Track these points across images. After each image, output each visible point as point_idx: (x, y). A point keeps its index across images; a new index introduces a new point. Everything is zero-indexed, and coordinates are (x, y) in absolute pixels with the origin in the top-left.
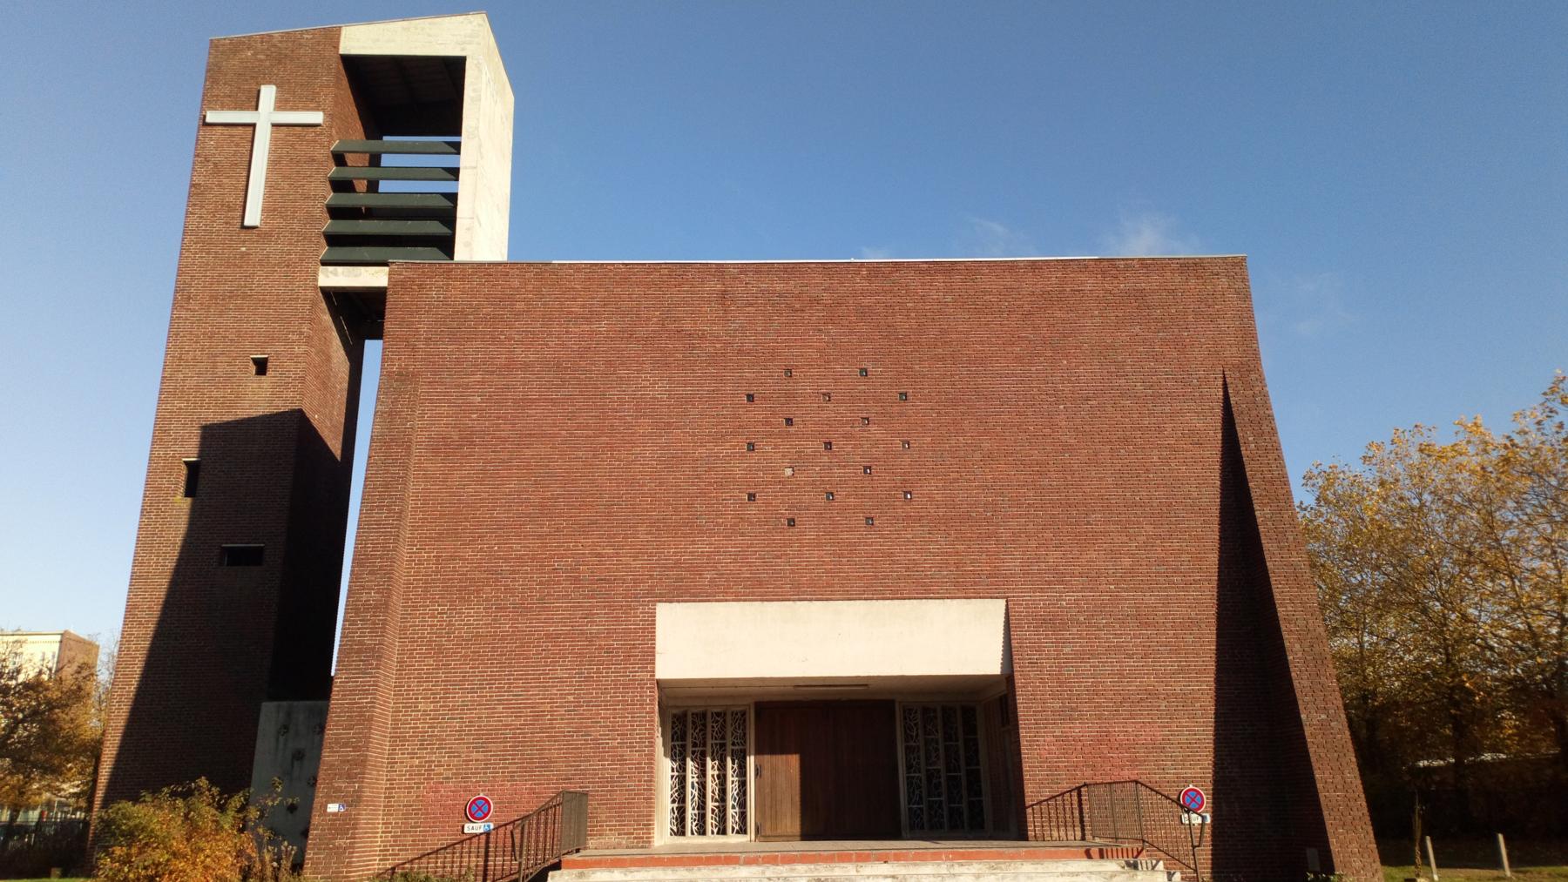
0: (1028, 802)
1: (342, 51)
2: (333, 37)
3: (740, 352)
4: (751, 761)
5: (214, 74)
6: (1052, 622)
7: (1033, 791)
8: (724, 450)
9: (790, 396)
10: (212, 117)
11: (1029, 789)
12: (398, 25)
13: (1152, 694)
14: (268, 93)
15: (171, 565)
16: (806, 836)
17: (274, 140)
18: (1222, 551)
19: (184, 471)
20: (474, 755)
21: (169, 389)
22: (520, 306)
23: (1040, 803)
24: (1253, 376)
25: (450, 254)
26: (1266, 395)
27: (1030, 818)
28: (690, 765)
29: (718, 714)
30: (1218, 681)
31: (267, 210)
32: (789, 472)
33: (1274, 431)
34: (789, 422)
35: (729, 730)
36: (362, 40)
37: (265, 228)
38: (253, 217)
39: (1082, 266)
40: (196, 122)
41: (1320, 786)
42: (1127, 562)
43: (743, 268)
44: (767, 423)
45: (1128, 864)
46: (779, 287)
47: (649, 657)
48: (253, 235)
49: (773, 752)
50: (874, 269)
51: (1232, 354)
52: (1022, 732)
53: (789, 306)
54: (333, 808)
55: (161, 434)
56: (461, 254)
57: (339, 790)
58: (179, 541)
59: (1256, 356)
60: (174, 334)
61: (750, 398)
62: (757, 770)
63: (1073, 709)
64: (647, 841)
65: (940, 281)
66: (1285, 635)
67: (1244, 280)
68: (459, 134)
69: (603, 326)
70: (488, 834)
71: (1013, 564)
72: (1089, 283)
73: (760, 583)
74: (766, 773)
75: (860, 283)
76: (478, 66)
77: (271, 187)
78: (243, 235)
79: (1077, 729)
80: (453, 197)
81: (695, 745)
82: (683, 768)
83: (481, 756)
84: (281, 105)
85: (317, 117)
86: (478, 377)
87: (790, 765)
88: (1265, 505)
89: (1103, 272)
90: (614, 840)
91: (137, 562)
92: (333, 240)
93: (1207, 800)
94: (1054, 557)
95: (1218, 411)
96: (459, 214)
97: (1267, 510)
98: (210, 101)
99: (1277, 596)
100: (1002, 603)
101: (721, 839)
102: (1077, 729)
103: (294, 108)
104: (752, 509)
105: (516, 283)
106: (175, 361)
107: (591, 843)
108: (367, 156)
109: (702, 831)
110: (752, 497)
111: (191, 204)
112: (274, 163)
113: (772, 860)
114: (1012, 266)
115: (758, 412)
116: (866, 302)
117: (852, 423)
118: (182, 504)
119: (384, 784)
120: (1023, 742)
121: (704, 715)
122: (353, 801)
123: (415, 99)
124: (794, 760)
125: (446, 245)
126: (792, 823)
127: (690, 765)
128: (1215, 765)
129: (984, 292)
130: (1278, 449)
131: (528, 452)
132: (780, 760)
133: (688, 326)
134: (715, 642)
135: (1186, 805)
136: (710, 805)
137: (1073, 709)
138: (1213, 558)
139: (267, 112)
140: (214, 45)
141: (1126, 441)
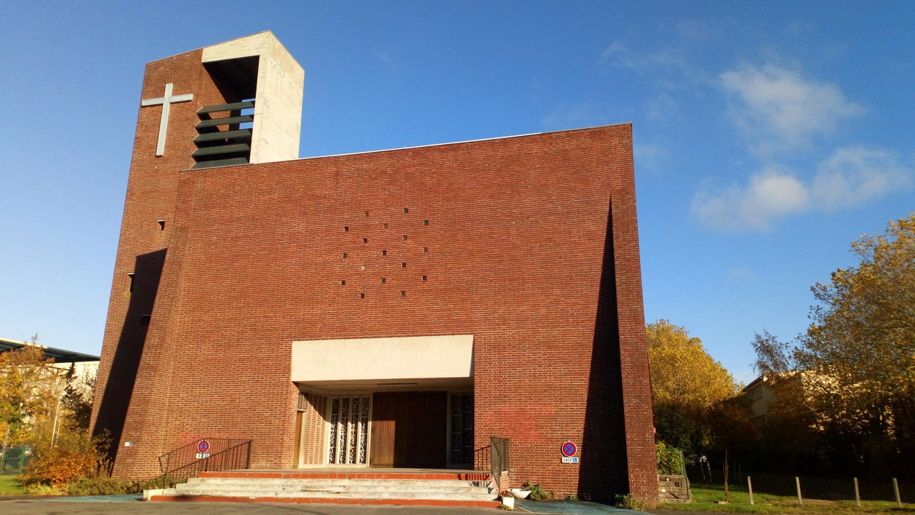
0: (476, 448)
1: (203, 61)
2: (199, 53)
3: (343, 204)
4: (370, 424)
5: (147, 81)
6: (498, 347)
7: (480, 440)
8: (330, 258)
9: (367, 226)
10: (144, 103)
11: (477, 441)
12: (228, 44)
13: (550, 387)
14: (169, 88)
15: (121, 325)
16: (397, 465)
17: (171, 111)
18: (600, 303)
19: (130, 279)
20: (203, 420)
21: (123, 242)
22: (237, 188)
23: (482, 449)
24: (628, 197)
25: (248, 160)
26: (635, 208)
27: (476, 458)
28: (340, 426)
29: (356, 399)
30: (591, 379)
31: (167, 147)
32: (363, 268)
33: (636, 229)
34: (366, 240)
35: (361, 408)
36: (214, 53)
37: (166, 156)
38: (160, 151)
39: (533, 139)
40: (138, 106)
41: (628, 442)
42: (543, 311)
43: (348, 158)
44: (354, 242)
45: (474, 483)
46: (365, 166)
47: (287, 370)
48: (160, 160)
49: (381, 419)
50: (416, 152)
51: (618, 184)
52: (476, 409)
53: (370, 177)
54: (127, 444)
55: (119, 263)
56: (253, 160)
57: (131, 436)
58: (125, 314)
59: (632, 183)
60: (126, 212)
61: (347, 229)
62: (445, 429)
63: (505, 397)
64: (280, 465)
65: (452, 153)
66: (622, 352)
67: (630, 138)
68: (254, 97)
70: (207, 459)
71: (478, 315)
72: (535, 149)
73: (345, 329)
74: (378, 432)
75: (408, 160)
76: (265, 59)
77: (169, 134)
78: (157, 161)
79: (505, 407)
80: (251, 130)
81: (344, 416)
82: (336, 428)
83: (206, 420)
84: (176, 92)
85: (190, 97)
87: (392, 424)
88: (623, 274)
89: (544, 142)
90: (264, 464)
91: (108, 325)
92: (198, 158)
93: (578, 449)
94: (501, 310)
95: (606, 219)
96: (253, 139)
97: (623, 277)
98: (145, 95)
99: (621, 329)
100: (471, 337)
101: (353, 466)
102: (505, 407)
103: (180, 94)
104: (343, 290)
106: (126, 226)
107: (253, 465)
108: (229, 112)
110: (344, 283)
112: (171, 122)
113: (379, 476)
114: (492, 143)
115: (349, 237)
116: (410, 171)
117: (398, 239)
118: (127, 294)
119: (163, 433)
120: (476, 415)
121: (325, 399)
122: (136, 441)
123: (237, 80)
124: (392, 424)
125: (246, 155)
126: (389, 458)
127: (340, 426)
128: (585, 429)
129: (476, 159)
130: (637, 240)
132: (385, 423)
133: (318, 192)
134: (321, 360)
135: (568, 450)
136: (349, 447)
137: (505, 397)
138: (595, 307)
139: (169, 95)
140: (147, 66)
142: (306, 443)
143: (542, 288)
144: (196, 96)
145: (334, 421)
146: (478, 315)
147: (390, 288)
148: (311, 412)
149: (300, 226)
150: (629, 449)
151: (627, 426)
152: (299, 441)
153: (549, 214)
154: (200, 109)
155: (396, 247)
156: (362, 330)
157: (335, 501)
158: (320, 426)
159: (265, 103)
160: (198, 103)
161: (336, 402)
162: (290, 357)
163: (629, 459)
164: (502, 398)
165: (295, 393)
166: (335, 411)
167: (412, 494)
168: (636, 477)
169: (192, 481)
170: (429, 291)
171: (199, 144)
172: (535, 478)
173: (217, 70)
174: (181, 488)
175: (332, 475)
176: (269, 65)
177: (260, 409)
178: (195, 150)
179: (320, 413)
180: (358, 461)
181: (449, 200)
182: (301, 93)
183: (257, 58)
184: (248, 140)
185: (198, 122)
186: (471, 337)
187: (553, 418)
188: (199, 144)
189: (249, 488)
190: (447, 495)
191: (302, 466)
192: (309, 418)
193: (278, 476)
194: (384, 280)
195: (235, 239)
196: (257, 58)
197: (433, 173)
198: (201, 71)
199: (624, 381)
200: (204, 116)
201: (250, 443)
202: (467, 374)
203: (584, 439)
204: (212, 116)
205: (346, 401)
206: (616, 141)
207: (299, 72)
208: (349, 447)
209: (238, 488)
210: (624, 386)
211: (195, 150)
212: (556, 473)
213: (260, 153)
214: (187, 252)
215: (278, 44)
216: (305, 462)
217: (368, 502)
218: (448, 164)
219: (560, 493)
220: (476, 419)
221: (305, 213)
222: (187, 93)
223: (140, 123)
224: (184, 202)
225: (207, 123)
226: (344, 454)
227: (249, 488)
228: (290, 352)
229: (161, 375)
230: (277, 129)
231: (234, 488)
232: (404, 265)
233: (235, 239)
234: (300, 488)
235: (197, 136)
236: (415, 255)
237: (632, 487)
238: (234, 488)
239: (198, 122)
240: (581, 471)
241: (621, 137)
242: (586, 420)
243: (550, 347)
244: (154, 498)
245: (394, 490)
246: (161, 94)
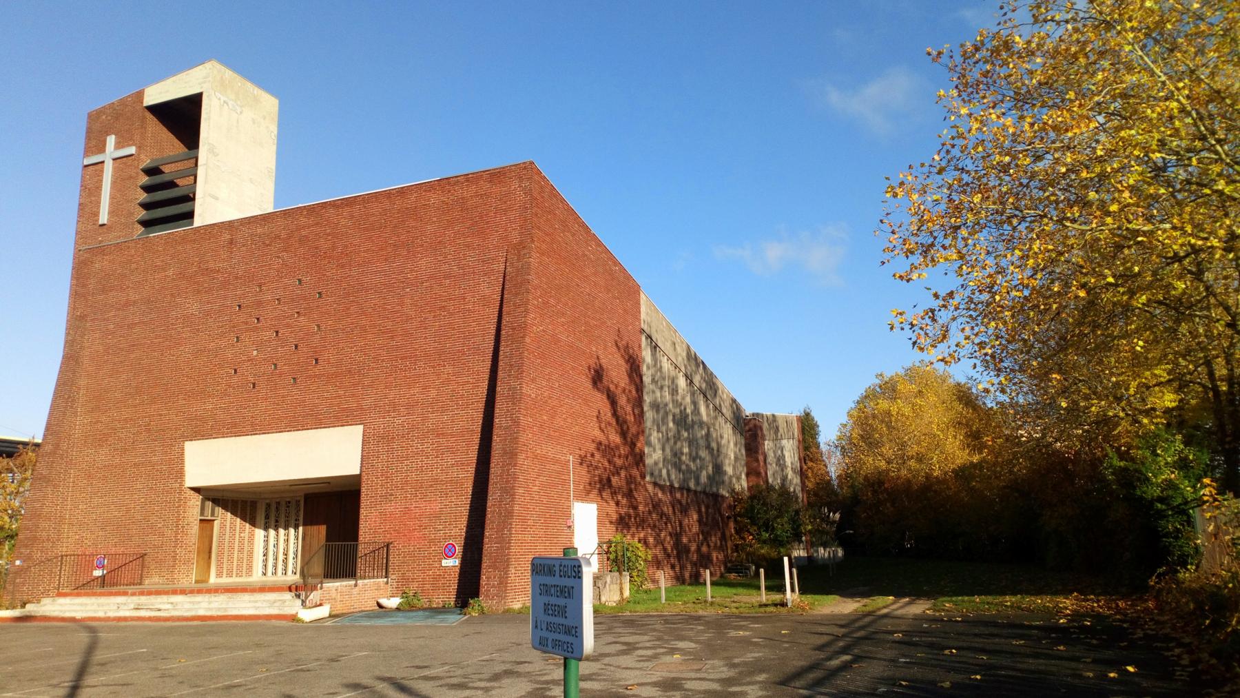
1: (145, 104)
2: (140, 95)
3: (237, 278)
9: (259, 304)
10: (86, 163)
12: (170, 81)
14: (111, 140)
17: (114, 168)
22: (134, 266)
32: (255, 353)
36: (158, 94)
38: (104, 218)
39: (429, 187)
41: (486, 540)
44: (246, 323)
46: (259, 231)
47: (180, 474)
50: (311, 210)
52: (362, 511)
56: (198, 222)
65: (347, 209)
66: (495, 437)
69: (170, 273)
72: (434, 199)
73: (235, 425)
74: (308, 538)
75: (303, 220)
77: (112, 198)
79: (389, 508)
84: (118, 146)
86: (112, 314)
87: (323, 529)
92: (147, 224)
93: (459, 550)
99: (497, 411)
101: (284, 578)
102: (389, 508)
103: (123, 147)
104: (235, 379)
105: (133, 252)
107: (147, 582)
109: (275, 573)
111: (80, 216)
112: (114, 183)
116: (303, 233)
125: (190, 215)
131: (132, 356)
133: (211, 265)
134: (216, 461)
140: (90, 116)
142: (218, 556)
143: (433, 367)
144: (139, 148)
145: (266, 529)
146: (368, 402)
147: (280, 375)
148: (224, 520)
149: (193, 307)
151: (487, 522)
152: (210, 552)
153: (445, 278)
154: (146, 162)
155: (288, 326)
156: (252, 425)
157: (150, 619)
158: (246, 535)
159: (212, 150)
160: (142, 156)
161: (268, 505)
162: (183, 460)
163: (485, 559)
164: (386, 497)
165: (196, 500)
166: (267, 517)
167: (225, 609)
169: (45, 601)
171: (146, 206)
174: (31, 608)
175: (263, 589)
177: (153, 519)
178: (142, 214)
179: (244, 519)
181: (343, 267)
182: (274, 129)
184: (190, 198)
185: (145, 180)
186: (361, 427)
187: (437, 516)
188: (146, 206)
189: (89, 608)
191: (213, 579)
192: (223, 526)
193: (175, 592)
194: (276, 365)
195: (131, 326)
197: (328, 235)
198: (144, 117)
199: (492, 471)
200: (152, 171)
201: (388, 546)
202: (358, 472)
203: (466, 538)
204: (166, 169)
205: (278, 503)
207: (270, 103)
208: (281, 557)
209: (78, 608)
210: (492, 476)
211: (142, 214)
212: (436, 578)
215: (228, 74)
216: (219, 575)
218: (343, 222)
219: (437, 601)
220: (361, 522)
221: (199, 292)
222: (129, 145)
223: (84, 187)
224: (84, 286)
225: (158, 179)
226: (275, 566)
227: (89, 608)
228: (183, 454)
229: (55, 486)
230: (237, 177)
232: (296, 346)
233: (131, 326)
234: (132, 606)
235: (143, 196)
237: (482, 590)
238: (74, 608)
239: (145, 180)
240: (460, 575)
241: (521, 179)
246: (101, 149)
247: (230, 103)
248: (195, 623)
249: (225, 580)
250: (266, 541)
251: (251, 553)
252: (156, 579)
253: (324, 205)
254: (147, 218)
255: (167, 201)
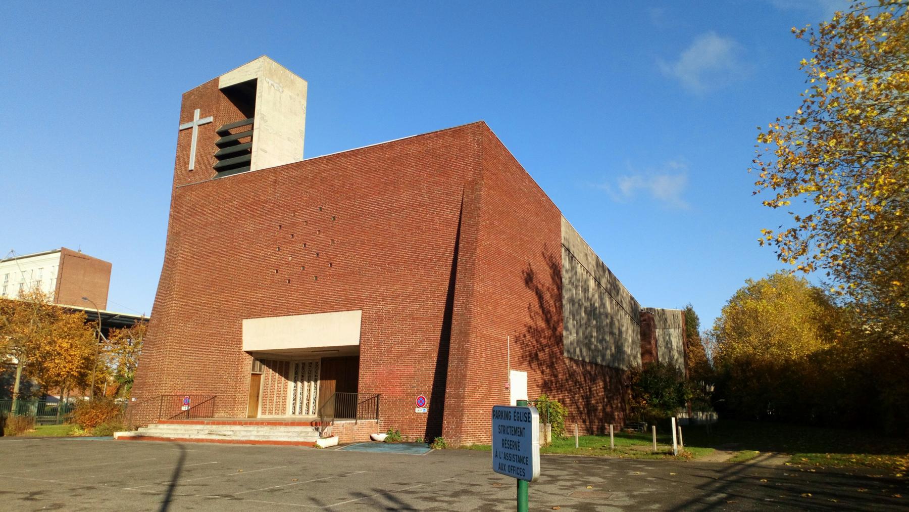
2: (216, 81)
6: (378, 320)
8: (269, 252)
9: (294, 224)
10: (181, 128)
13: (412, 352)
14: (197, 113)
24: (478, 186)
31: (197, 162)
36: (229, 79)
38: (192, 166)
39: (410, 141)
41: (447, 395)
42: (410, 288)
47: (239, 342)
50: (329, 158)
52: (360, 371)
56: (253, 168)
65: (353, 158)
66: (454, 321)
69: (235, 203)
71: (365, 294)
72: (412, 149)
73: (276, 309)
74: (323, 389)
77: (197, 152)
84: (202, 116)
85: (211, 119)
92: (220, 169)
93: (427, 401)
94: (381, 289)
98: (181, 123)
99: (455, 302)
101: (307, 416)
102: (379, 369)
104: (277, 277)
107: (216, 415)
109: (301, 413)
111: (176, 165)
112: (199, 142)
116: (323, 175)
120: (360, 375)
125: (248, 163)
131: (209, 260)
133: (262, 198)
134: (264, 333)
140: (184, 96)
141: (418, 228)
142: (265, 398)
144: (215, 118)
145: (295, 381)
146: (365, 294)
147: (307, 274)
148: (268, 374)
149: (250, 226)
150: (447, 400)
151: (448, 382)
152: (258, 397)
153: (420, 206)
154: (219, 127)
155: (312, 240)
157: (219, 441)
158: (282, 385)
159: (262, 118)
160: (217, 123)
161: (297, 365)
162: (241, 332)
163: (446, 409)
165: (249, 360)
166: (296, 373)
167: (268, 437)
168: (448, 423)
169: (151, 426)
170: (333, 276)
171: (219, 157)
172: (397, 425)
173: (230, 92)
175: (293, 423)
176: (265, 85)
178: (216, 163)
179: (281, 374)
180: (297, 413)
181: (349, 199)
182: (304, 103)
183: (256, 80)
184: (248, 152)
185: (218, 139)
186: (360, 312)
188: (219, 157)
190: (289, 437)
191: (260, 416)
192: (266, 379)
193: (235, 423)
195: (209, 239)
196: (256, 80)
198: (219, 96)
199: (451, 345)
200: (223, 133)
202: (358, 343)
203: (433, 393)
204: (232, 132)
205: (304, 364)
206: (471, 138)
207: (301, 85)
208: (305, 402)
210: (451, 350)
211: (216, 163)
212: (412, 421)
213: (260, 161)
214: (180, 252)
215: (275, 65)
216: (264, 413)
217: (259, 442)
218: (350, 167)
219: (412, 438)
220: (360, 379)
221: (254, 216)
224: (179, 212)
228: (241, 328)
229: (158, 348)
230: (280, 137)
231: (169, 431)
233: (209, 239)
235: (217, 151)
236: (325, 246)
237: (444, 431)
238: (169, 431)
239: (218, 139)
240: (428, 420)
242: (435, 378)
243: (413, 319)
244: (119, 438)
245: (261, 433)
246: (191, 119)
247: (276, 85)
248: (248, 445)
249: (267, 417)
250: (295, 390)
251: (285, 398)
252: (222, 414)
253: (338, 156)
254: (220, 165)
255: (233, 153)
